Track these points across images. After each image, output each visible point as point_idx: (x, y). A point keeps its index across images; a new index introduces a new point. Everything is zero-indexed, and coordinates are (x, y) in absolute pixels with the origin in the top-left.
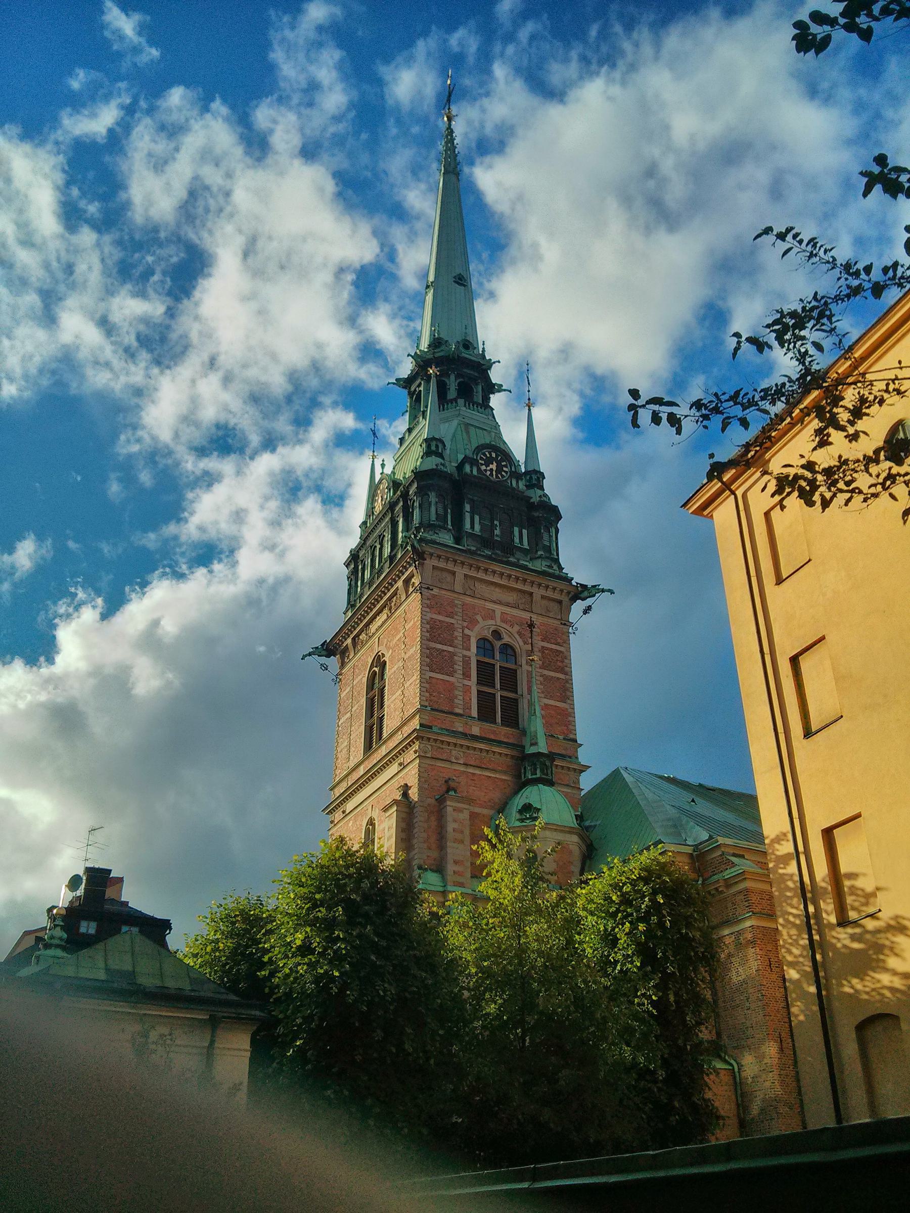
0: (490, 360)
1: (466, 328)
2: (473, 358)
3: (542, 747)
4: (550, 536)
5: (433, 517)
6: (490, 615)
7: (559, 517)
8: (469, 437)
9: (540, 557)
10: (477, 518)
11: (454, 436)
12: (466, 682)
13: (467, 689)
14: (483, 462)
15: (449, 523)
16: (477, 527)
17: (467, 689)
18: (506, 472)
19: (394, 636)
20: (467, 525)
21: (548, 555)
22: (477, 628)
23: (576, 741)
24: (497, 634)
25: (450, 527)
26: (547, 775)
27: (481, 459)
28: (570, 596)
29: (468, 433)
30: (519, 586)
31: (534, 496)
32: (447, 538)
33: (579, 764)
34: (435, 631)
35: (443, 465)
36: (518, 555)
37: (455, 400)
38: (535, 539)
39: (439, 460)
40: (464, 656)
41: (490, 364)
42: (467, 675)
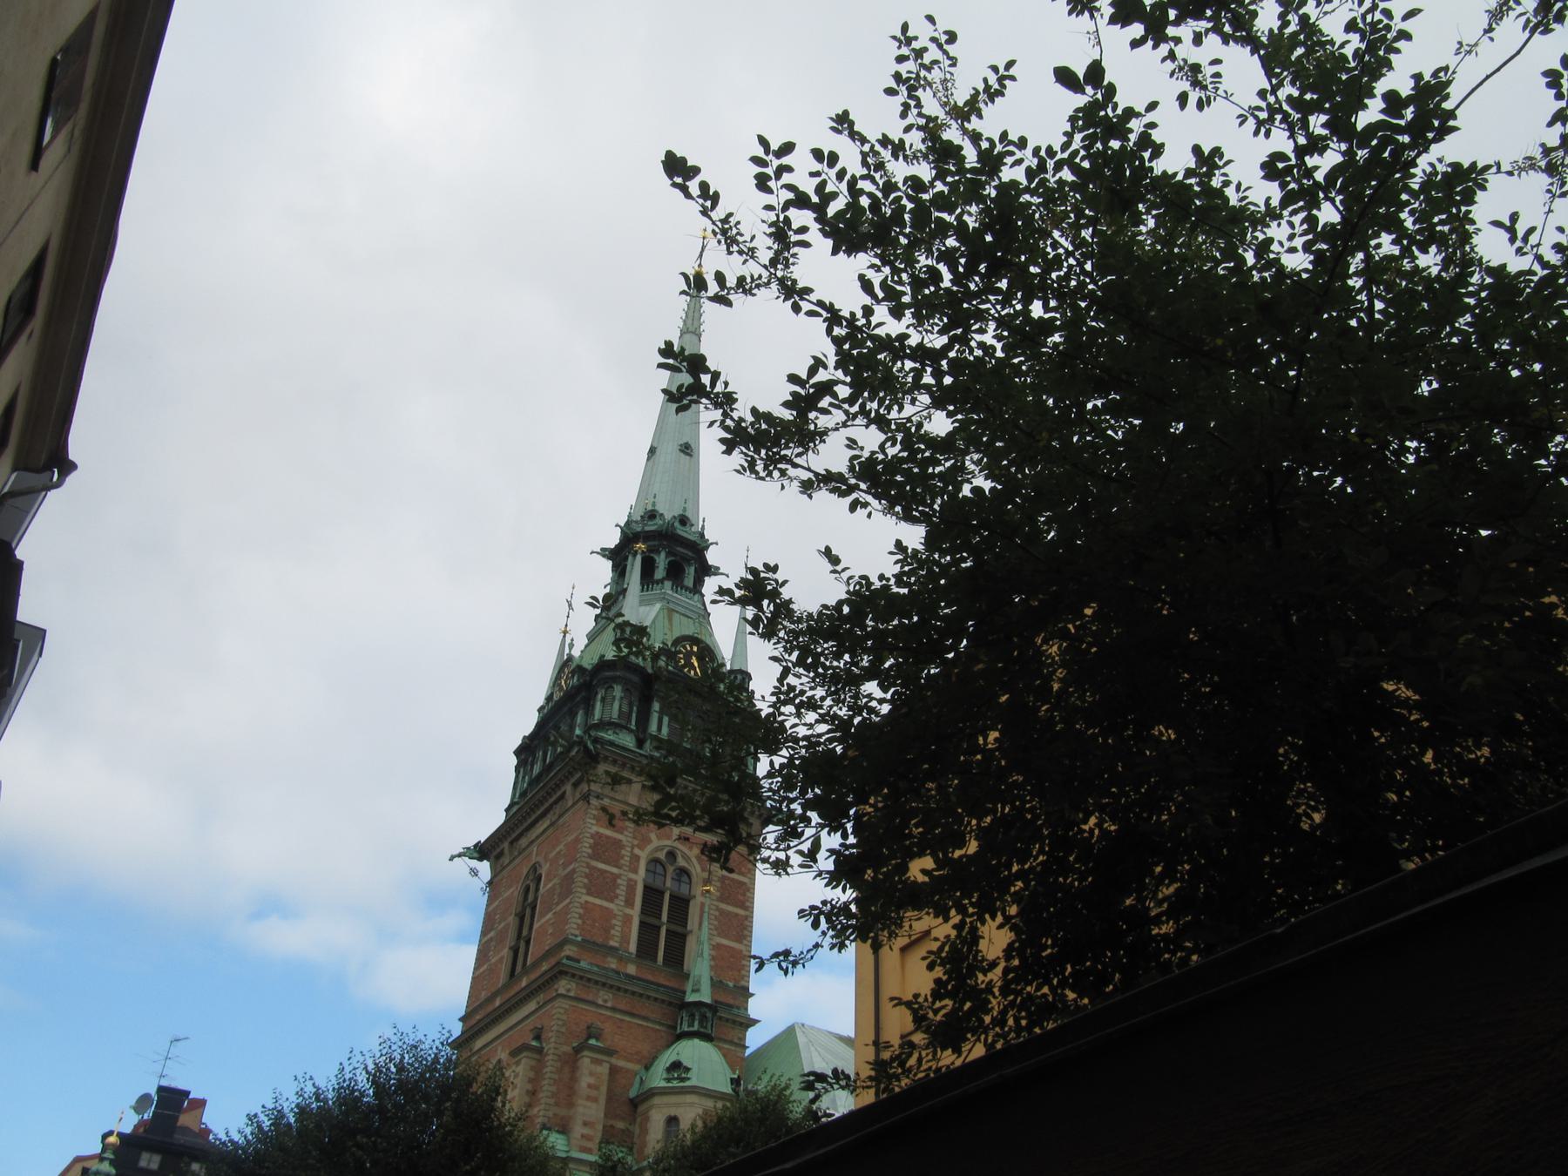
3: (705, 996)
5: (615, 714)
8: (671, 624)
12: (628, 911)
13: (627, 920)
15: (633, 722)
16: (665, 730)
17: (627, 920)
20: (653, 728)
22: (649, 848)
24: (672, 855)
25: (633, 727)
26: (706, 1028)
28: (762, 819)
29: (670, 620)
32: (627, 740)
34: (599, 847)
37: (661, 581)
40: (630, 880)
42: (629, 903)
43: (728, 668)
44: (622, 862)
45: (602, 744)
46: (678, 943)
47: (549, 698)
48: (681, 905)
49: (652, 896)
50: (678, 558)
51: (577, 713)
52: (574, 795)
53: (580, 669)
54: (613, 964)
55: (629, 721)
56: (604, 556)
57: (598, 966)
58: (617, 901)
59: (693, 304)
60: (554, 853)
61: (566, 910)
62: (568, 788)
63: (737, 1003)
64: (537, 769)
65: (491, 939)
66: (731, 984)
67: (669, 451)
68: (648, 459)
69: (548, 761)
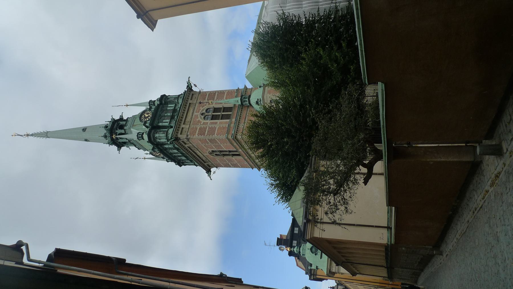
0: (111, 119)
1: (101, 127)
2: (111, 125)
3: (239, 99)
4: (171, 97)
5: (164, 135)
6: (197, 117)
7: (165, 95)
8: (137, 125)
9: (178, 101)
11: (136, 130)
12: (218, 123)
13: (220, 123)
14: (146, 119)
15: (166, 130)
17: (220, 123)
18: (149, 112)
19: (204, 148)
20: (167, 124)
21: (177, 98)
22: (201, 120)
23: (237, 89)
24: (202, 114)
25: (167, 130)
27: (144, 120)
29: (136, 125)
30: (187, 107)
31: (157, 103)
32: (171, 131)
33: (244, 88)
34: (201, 133)
35: (146, 132)
36: (177, 108)
37: (125, 130)
38: (171, 102)
39: (145, 133)
40: (210, 124)
41: (113, 119)
43: (149, 107)
44: (205, 127)
45: (172, 136)
46: (225, 109)
47: (163, 158)
48: (216, 110)
49: (214, 118)
50: (118, 127)
51: (165, 148)
52: (188, 144)
53: (153, 149)
54: (232, 125)
55: (165, 131)
56: (120, 150)
57: (233, 129)
58: (216, 127)
59: (37, 135)
60: (205, 147)
61: (219, 140)
62: (186, 146)
63: (241, 92)
64: (184, 158)
65: (231, 164)
66: (236, 94)
67: (85, 135)
68: (89, 141)
69: (181, 155)
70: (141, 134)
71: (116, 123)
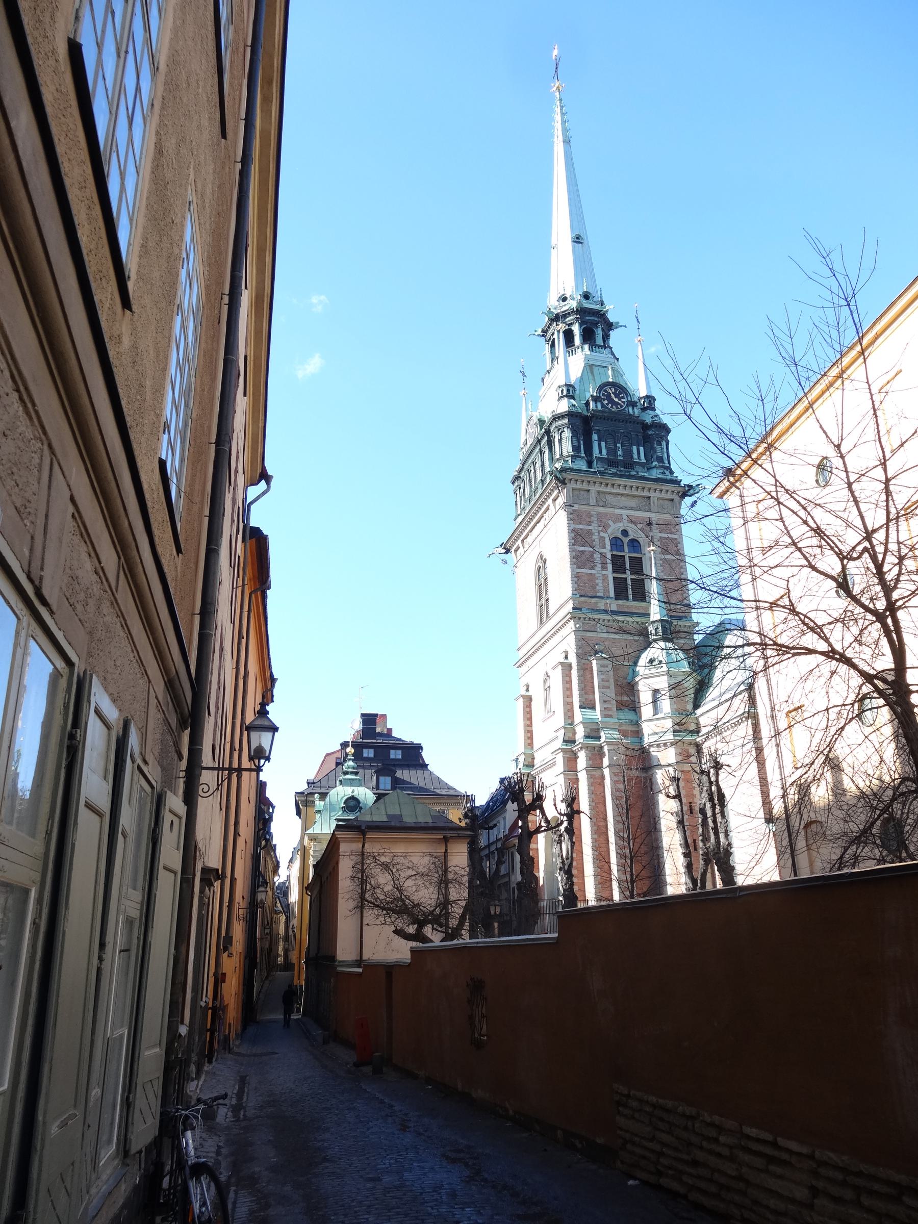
10: (603, 444)
24: (625, 533)
25: (583, 455)
31: (648, 418)
36: (638, 468)
70: (571, 394)
71: (598, 317)
